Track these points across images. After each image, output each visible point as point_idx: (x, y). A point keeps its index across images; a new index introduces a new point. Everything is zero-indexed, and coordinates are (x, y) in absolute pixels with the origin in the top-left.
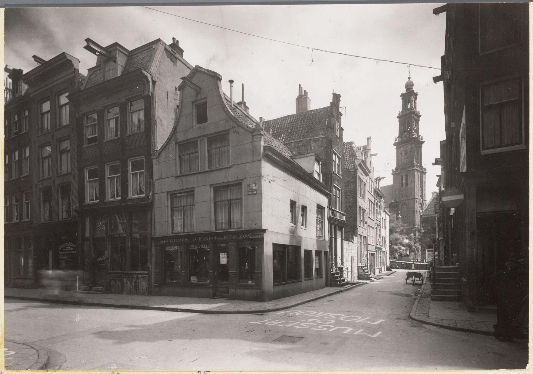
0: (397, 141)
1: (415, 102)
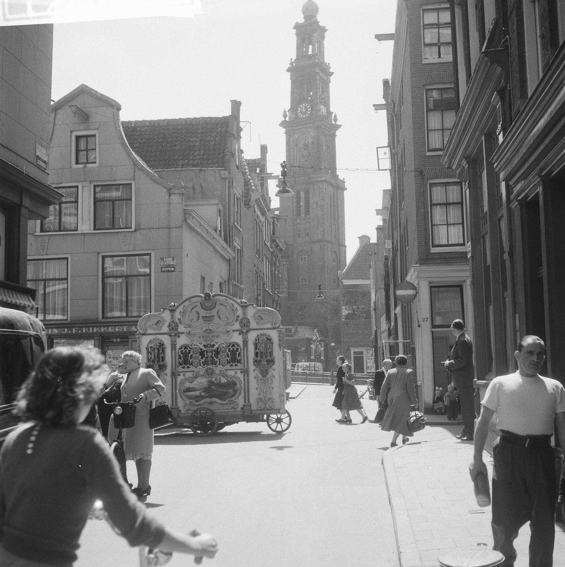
0: (287, 119)
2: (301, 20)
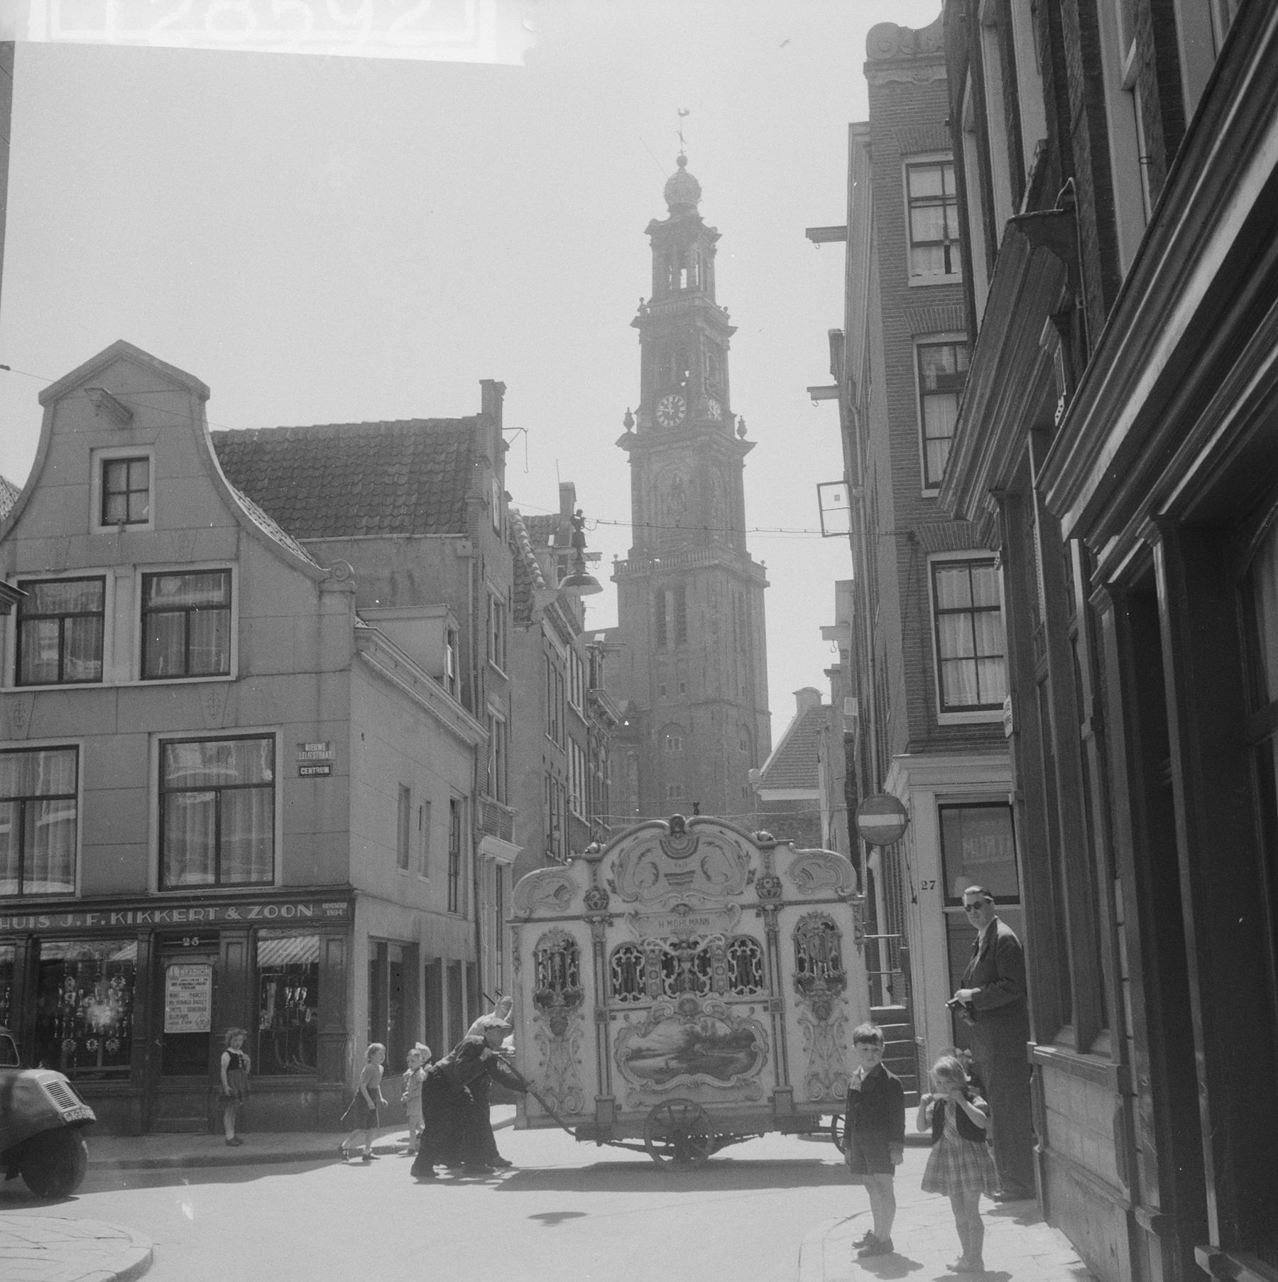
0: (634, 430)
1: (707, 269)
2: (663, 215)
